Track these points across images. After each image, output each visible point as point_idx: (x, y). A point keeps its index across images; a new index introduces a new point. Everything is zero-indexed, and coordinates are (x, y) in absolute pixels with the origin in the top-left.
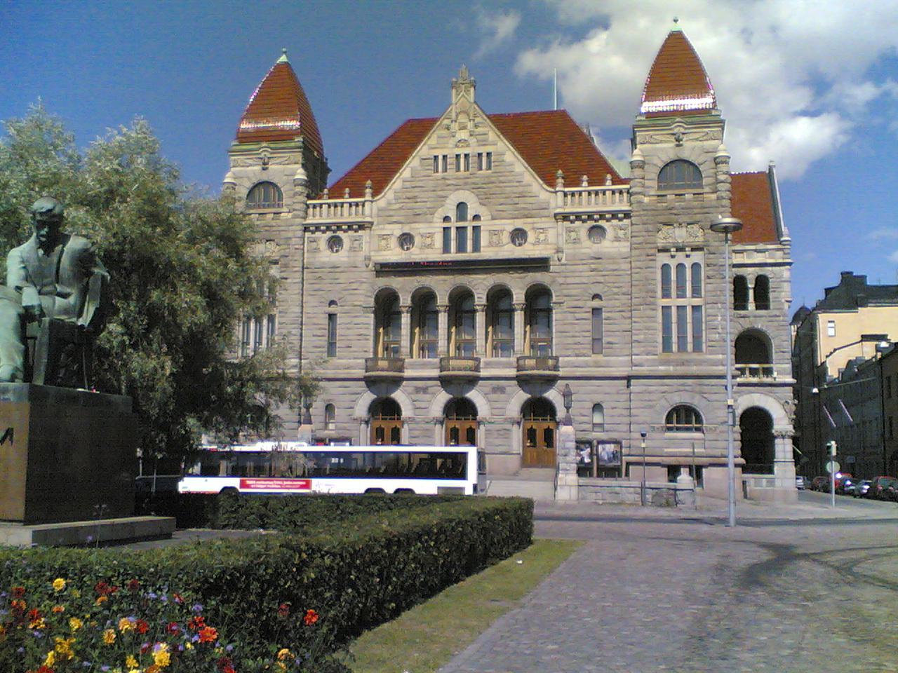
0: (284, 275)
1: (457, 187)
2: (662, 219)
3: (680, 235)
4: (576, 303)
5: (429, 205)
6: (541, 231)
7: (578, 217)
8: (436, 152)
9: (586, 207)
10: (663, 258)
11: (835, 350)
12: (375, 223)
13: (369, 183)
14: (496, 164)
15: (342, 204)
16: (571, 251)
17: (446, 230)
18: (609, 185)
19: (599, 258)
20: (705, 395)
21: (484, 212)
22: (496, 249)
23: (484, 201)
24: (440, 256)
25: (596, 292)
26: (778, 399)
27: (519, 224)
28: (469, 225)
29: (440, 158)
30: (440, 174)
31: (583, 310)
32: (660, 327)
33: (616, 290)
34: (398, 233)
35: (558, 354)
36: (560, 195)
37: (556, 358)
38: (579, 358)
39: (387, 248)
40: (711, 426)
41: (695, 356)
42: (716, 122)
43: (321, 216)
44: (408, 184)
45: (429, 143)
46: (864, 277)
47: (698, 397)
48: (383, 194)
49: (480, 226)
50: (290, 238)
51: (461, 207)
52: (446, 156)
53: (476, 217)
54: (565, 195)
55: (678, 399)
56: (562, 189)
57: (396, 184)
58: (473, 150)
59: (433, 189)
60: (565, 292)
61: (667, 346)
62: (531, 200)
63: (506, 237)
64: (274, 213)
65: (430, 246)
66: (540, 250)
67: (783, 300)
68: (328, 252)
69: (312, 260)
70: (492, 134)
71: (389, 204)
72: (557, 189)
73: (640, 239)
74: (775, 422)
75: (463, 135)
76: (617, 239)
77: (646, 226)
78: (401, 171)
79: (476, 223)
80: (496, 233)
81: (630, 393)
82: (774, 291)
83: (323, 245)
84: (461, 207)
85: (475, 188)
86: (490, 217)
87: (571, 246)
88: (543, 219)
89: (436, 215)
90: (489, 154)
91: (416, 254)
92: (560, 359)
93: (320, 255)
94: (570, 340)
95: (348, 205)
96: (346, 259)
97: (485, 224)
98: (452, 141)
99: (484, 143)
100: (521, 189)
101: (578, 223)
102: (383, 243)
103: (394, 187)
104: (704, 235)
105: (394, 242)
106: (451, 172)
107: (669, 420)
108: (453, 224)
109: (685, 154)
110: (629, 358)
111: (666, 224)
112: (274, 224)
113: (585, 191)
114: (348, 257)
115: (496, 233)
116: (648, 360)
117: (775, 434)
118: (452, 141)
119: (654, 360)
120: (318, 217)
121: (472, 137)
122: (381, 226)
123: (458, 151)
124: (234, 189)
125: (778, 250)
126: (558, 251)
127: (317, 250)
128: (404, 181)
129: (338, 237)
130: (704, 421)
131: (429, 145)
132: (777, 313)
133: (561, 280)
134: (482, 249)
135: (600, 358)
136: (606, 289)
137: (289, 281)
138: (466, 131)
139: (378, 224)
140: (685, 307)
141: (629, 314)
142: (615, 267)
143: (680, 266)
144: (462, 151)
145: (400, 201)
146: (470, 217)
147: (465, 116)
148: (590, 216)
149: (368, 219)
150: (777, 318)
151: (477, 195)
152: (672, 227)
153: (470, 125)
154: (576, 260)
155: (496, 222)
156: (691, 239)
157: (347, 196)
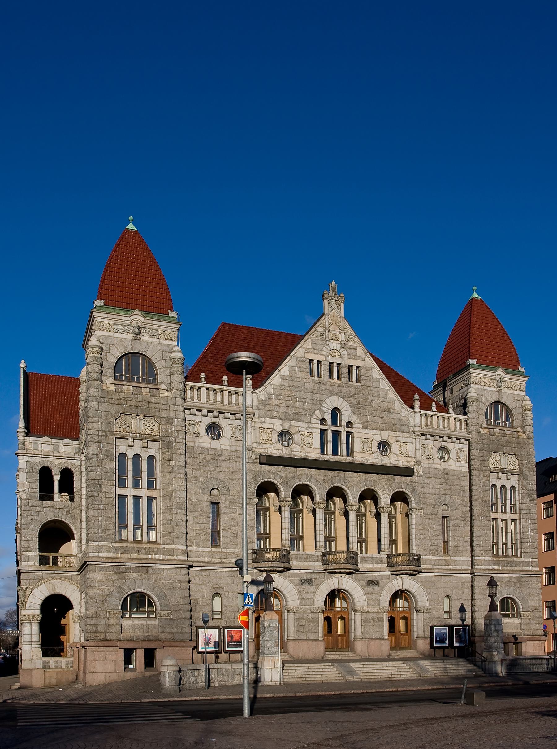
0: (167, 456)
1: (332, 394)
5: (306, 406)
6: (402, 444)
10: (493, 479)
12: (256, 415)
14: (366, 378)
17: (323, 432)
22: (366, 455)
23: (356, 408)
24: (318, 455)
27: (385, 435)
28: (344, 430)
33: (459, 502)
34: (279, 429)
36: (417, 415)
39: (270, 442)
44: (286, 383)
45: (305, 346)
48: (263, 387)
51: (335, 412)
52: (321, 361)
53: (349, 424)
56: (419, 410)
57: (275, 379)
59: (311, 391)
63: (375, 448)
65: (310, 445)
68: (208, 439)
70: (361, 351)
72: (415, 410)
73: (478, 463)
75: (335, 345)
76: (459, 460)
78: (280, 368)
84: (335, 412)
86: (361, 426)
88: (404, 434)
89: (314, 416)
90: (358, 367)
91: (297, 452)
93: (201, 440)
96: (228, 448)
98: (325, 351)
99: (355, 357)
100: (386, 404)
102: (265, 436)
105: (275, 436)
108: (330, 428)
114: (230, 446)
115: (366, 440)
121: (343, 349)
122: (262, 419)
126: (418, 463)
127: (196, 435)
131: (304, 348)
134: (355, 454)
138: (338, 342)
139: (259, 417)
143: (503, 486)
144: (336, 361)
145: (279, 398)
151: (350, 404)
153: (342, 337)
154: (430, 473)
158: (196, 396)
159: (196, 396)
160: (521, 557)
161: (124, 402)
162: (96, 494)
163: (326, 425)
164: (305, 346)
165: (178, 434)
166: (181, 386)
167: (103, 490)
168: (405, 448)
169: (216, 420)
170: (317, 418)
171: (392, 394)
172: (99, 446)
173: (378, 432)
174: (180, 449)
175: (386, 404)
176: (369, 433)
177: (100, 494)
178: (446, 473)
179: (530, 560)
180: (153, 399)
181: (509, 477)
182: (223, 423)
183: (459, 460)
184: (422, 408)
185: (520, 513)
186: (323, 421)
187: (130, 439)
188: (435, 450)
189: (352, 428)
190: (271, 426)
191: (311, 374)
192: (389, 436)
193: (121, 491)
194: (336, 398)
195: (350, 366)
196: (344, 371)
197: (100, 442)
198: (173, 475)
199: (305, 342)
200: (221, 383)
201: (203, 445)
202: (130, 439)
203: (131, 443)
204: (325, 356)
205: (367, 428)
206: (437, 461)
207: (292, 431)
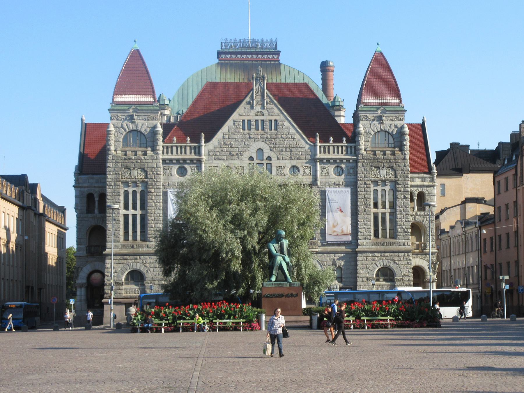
2: (376, 164)
3: (384, 172)
7: (328, 161)
8: (243, 118)
9: (332, 155)
13: (203, 135)
15: (186, 147)
21: (273, 155)
23: (273, 147)
27: (294, 163)
32: (372, 224)
42: (402, 111)
43: (172, 153)
46: (468, 146)
49: (271, 164)
51: (260, 151)
53: (269, 158)
57: (219, 135)
58: (267, 118)
61: (376, 235)
64: (142, 151)
79: (269, 162)
83: (174, 171)
84: (260, 151)
85: (266, 140)
87: (323, 177)
90: (276, 121)
93: (172, 177)
95: (189, 147)
97: (275, 163)
106: (253, 130)
107: (377, 275)
111: (375, 167)
112: (143, 158)
113: (331, 146)
118: (253, 112)
120: (170, 154)
121: (265, 110)
122: (211, 161)
128: (223, 134)
144: (260, 118)
146: (265, 158)
155: (281, 161)
158: (170, 152)
159: (170, 152)
163: (253, 160)
164: (239, 112)
170: (246, 156)
173: (289, 161)
175: (295, 142)
176: (282, 163)
181: (387, 184)
182: (186, 166)
186: (251, 158)
187: (130, 182)
189: (271, 160)
193: (126, 212)
195: (270, 121)
200: (186, 142)
201: (174, 181)
204: (253, 116)
207: (231, 166)
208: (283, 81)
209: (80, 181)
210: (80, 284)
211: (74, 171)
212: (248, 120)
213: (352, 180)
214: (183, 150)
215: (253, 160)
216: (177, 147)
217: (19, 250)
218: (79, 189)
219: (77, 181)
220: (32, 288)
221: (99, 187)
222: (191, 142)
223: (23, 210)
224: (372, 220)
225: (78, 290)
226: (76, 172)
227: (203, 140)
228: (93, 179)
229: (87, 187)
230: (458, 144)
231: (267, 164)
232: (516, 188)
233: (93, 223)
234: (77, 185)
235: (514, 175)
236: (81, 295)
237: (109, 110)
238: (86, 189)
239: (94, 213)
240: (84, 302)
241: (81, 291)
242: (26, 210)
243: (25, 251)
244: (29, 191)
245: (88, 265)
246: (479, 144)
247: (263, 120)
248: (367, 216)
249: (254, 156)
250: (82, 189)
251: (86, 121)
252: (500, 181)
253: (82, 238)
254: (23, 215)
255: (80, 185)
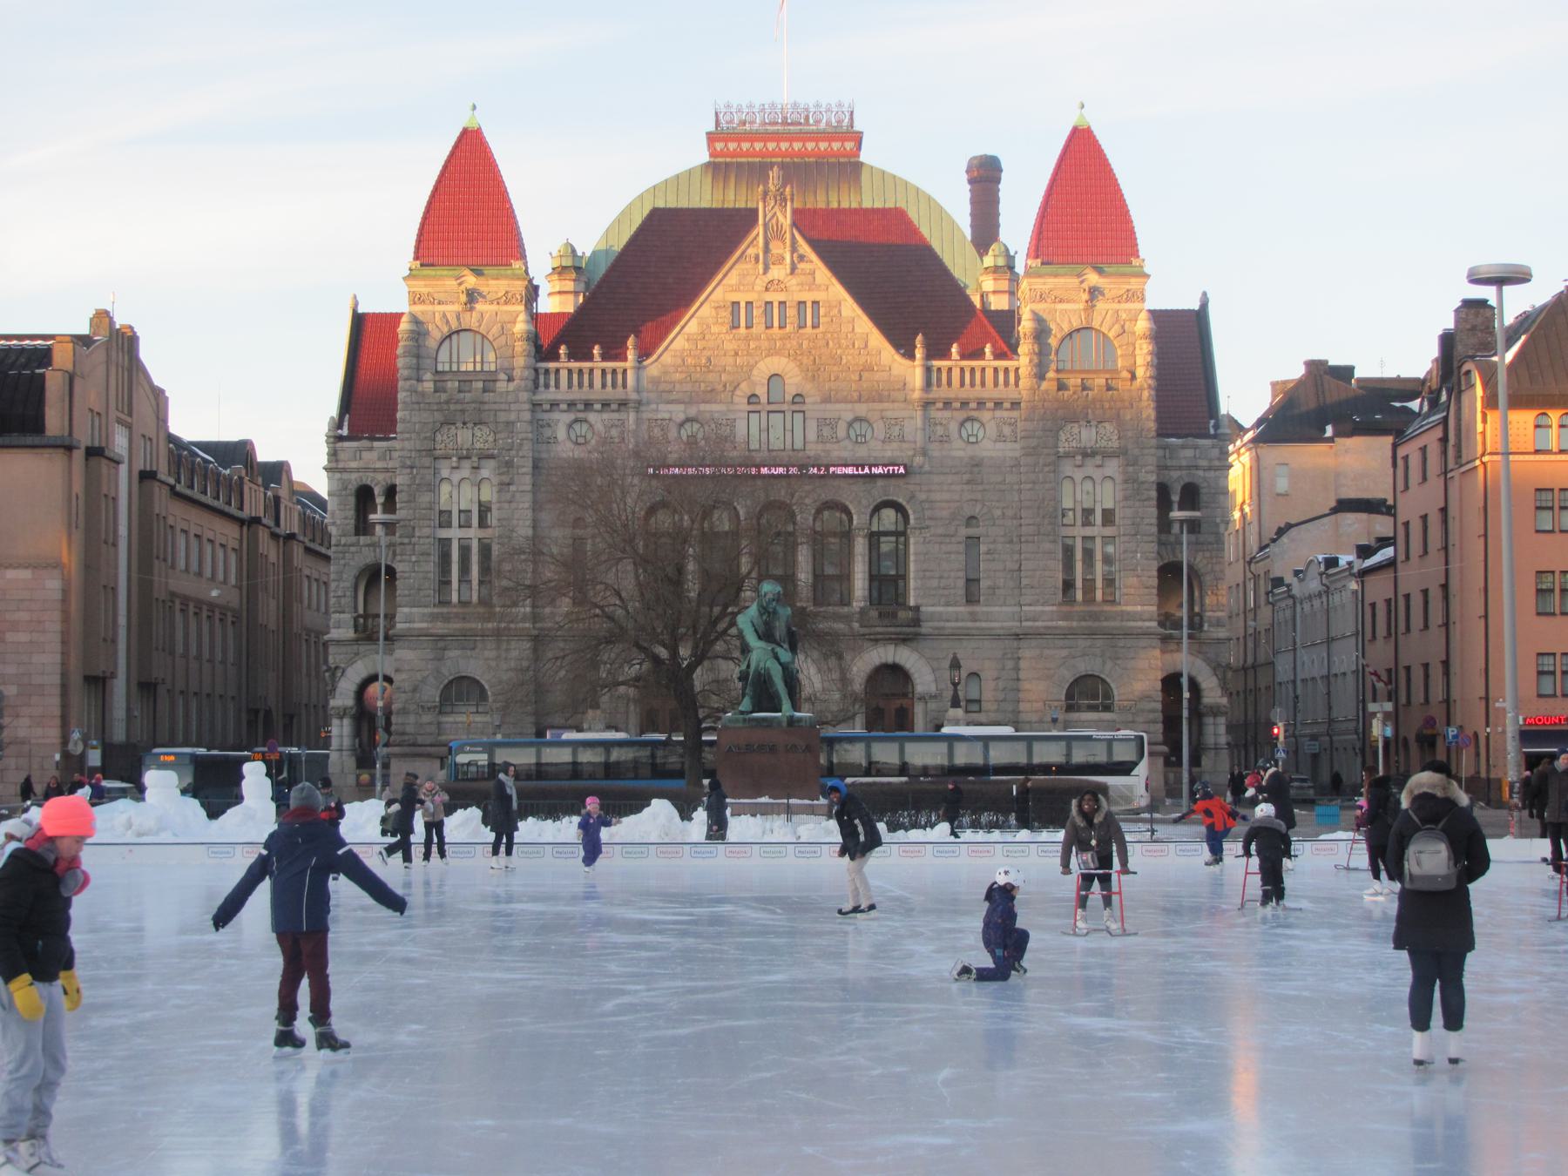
0: (506, 479)
4: (940, 531)
11: (1289, 526)
12: (644, 401)
16: (936, 454)
18: (989, 361)
19: (977, 465)
20: (1119, 662)
25: (969, 514)
26: (1208, 661)
29: (743, 305)
30: (742, 330)
31: (953, 539)
33: (998, 513)
35: (920, 602)
37: (917, 609)
38: (950, 609)
40: (1125, 703)
41: (1107, 608)
45: (725, 282)
47: (1109, 664)
48: (655, 357)
50: (513, 423)
52: (752, 303)
54: (928, 370)
55: (1083, 667)
60: (928, 513)
62: (877, 376)
64: (484, 381)
66: (892, 450)
67: (1218, 520)
69: (544, 455)
70: (823, 274)
71: (666, 373)
73: (1034, 442)
74: (1205, 693)
76: (1001, 438)
77: (1041, 423)
80: (828, 422)
81: (1019, 658)
82: (1207, 507)
88: (896, 405)
89: (738, 392)
90: (816, 303)
92: (923, 609)
93: (559, 448)
94: (935, 583)
98: (760, 284)
99: (812, 286)
100: (862, 360)
101: (947, 414)
103: (675, 345)
104: (1119, 438)
106: (759, 327)
107: (1069, 695)
109: (1096, 324)
110: (1017, 609)
112: (486, 399)
115: (828, 422)
116: (1043, 612)
117: (1204, 710)
119: (1052, 611)
120: (552, 389)
122: (653, 406)
123: (769, 297)
124: (417, 341)
125: (1213, 447)
129: (586, 421)
130: (1116, 698)
132: (1211, 538)
133: (923, 496)
135: (977, 609)
136: (985, 510)
137: (512, 488)
140: (1093, 538)
141: (1017, 547)
142: (1000, 479)
145: (679, 369)
147: (780, 243)
148: (964, 404)
149: (634, 396)
150: (1210, 547)
152: (1076, 425)
155: (829, 406)
156: (1103, 443)
157: (597, 357)
158: (552, 383)
159: (552, 383)
160: (1120, 604)
161: (445, 407)
162: (406, 541)
163: (759, 403)
165: (521, 445)
166: (529, 373)
167: (417, 534)
168: (897, 428)
169: (581, 415)
171: (877, 339)
172: (411, 473)
173: (849, 406)
174: (524, 467)
177: (413, 540)
178: (976, 464)
179: (1139, 608)
180: (488, 397)
183: (1001, 438)
184: (930, 356)
185: (1119, 526)
188: (954, 427)
190: (667, 416)
191: (735, 326)
192: (869, 411)
193: (444, 533)
194: (776, 359)
195: (801, 303)
196: (791, 312)
197: (412, 467)
198: (514, 505)
199: (725, 276)
200: (590, 358)
202: (454, 459)
203: (454, 465)
204: (759, 292)
205: (830, 402)
206: (958, 444)
208: (867, 204)
209: (342, 456)
210: (338, 708)
211: (327, 430)
212: (747, 303)
213: (1011, 454)
214: (586, 377)
215: (759, 403)
216: (570, 371)
217: (229, 623)
218: (338, 475)
219: (333, 455)
220: (268, 713)
221: (386, 470)
222: (605, 358)
223: (241, 526)
224: (1060, 556)
225: (335, 722)
226: (331, 434)
227: (631, 355)
228: (371, 449)
229: (358, 470)
230: (1323, 363)
231: (793, 412)
232: (1445, 473)
233: (367, 558)
234: (334, 465)
235: (1440, 440)
236: (341, 736)
237: (405, 279)
238: (354, 476)
239: (373, 534)
240: (349, 753)
241: (342, 726)
242: (249, 527)
243: (244, 629)
244: (260, 480)
245: (359, 662)
246: (1382, 364)
247: (785, 303)
248: (1047, 546)
249: (761, 391)
250: (345, 476)
251: (360, 310)
252: (1407, 456)
253: (344, 596)
254: (241, 535)
255: (341, 465)
